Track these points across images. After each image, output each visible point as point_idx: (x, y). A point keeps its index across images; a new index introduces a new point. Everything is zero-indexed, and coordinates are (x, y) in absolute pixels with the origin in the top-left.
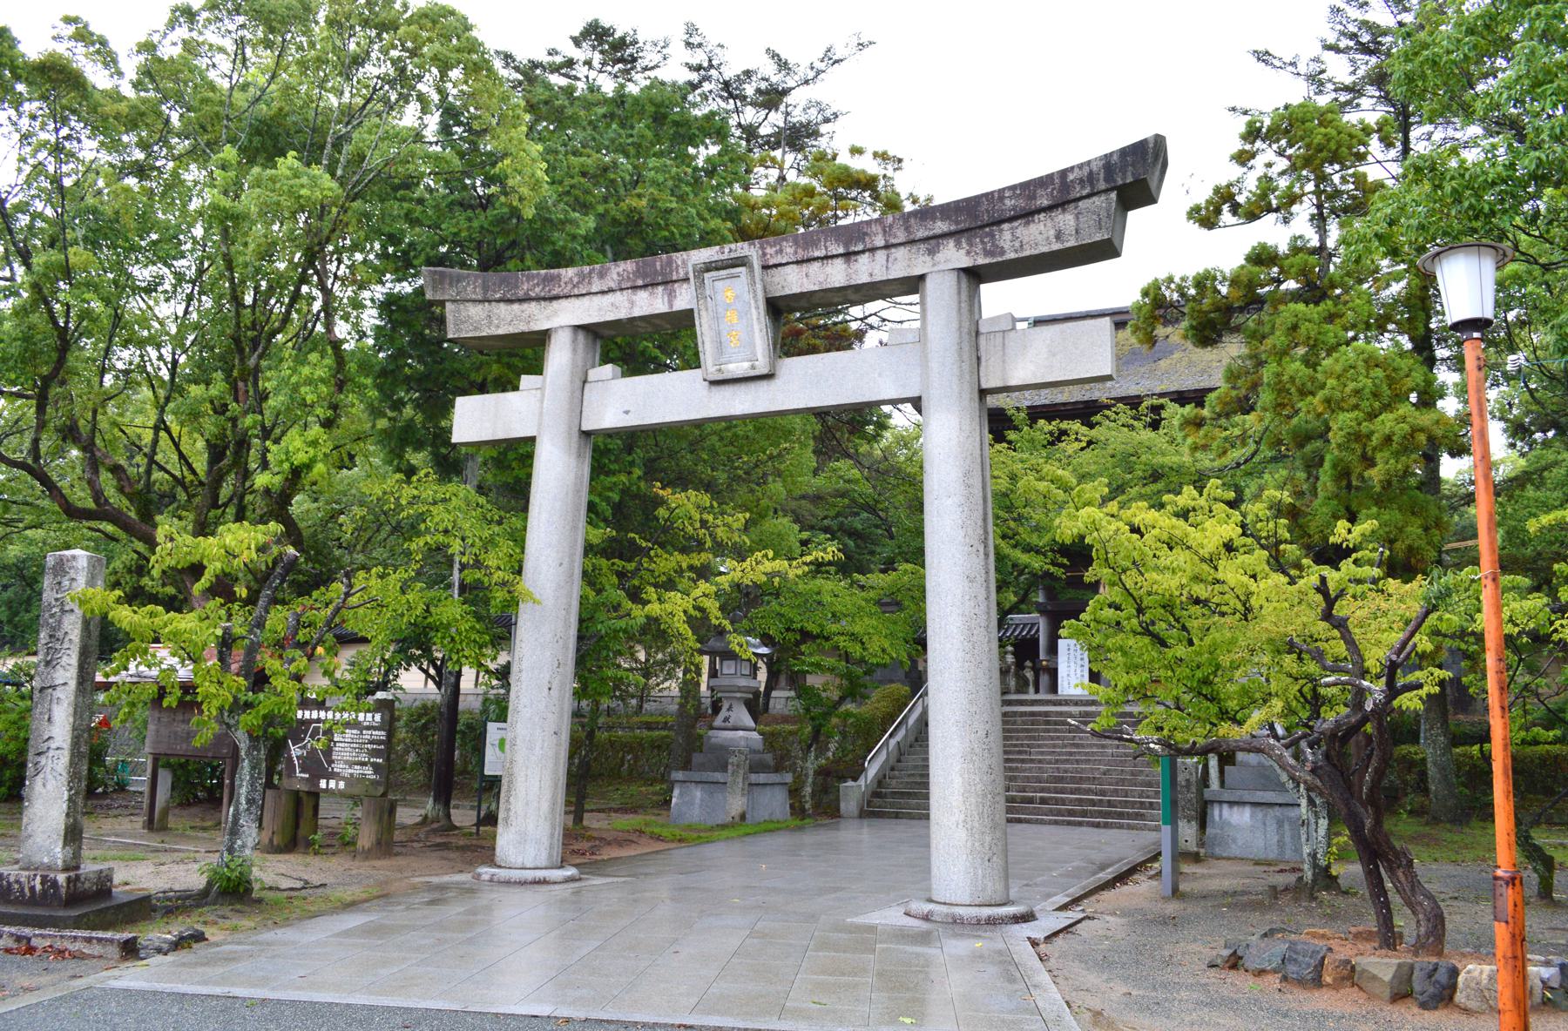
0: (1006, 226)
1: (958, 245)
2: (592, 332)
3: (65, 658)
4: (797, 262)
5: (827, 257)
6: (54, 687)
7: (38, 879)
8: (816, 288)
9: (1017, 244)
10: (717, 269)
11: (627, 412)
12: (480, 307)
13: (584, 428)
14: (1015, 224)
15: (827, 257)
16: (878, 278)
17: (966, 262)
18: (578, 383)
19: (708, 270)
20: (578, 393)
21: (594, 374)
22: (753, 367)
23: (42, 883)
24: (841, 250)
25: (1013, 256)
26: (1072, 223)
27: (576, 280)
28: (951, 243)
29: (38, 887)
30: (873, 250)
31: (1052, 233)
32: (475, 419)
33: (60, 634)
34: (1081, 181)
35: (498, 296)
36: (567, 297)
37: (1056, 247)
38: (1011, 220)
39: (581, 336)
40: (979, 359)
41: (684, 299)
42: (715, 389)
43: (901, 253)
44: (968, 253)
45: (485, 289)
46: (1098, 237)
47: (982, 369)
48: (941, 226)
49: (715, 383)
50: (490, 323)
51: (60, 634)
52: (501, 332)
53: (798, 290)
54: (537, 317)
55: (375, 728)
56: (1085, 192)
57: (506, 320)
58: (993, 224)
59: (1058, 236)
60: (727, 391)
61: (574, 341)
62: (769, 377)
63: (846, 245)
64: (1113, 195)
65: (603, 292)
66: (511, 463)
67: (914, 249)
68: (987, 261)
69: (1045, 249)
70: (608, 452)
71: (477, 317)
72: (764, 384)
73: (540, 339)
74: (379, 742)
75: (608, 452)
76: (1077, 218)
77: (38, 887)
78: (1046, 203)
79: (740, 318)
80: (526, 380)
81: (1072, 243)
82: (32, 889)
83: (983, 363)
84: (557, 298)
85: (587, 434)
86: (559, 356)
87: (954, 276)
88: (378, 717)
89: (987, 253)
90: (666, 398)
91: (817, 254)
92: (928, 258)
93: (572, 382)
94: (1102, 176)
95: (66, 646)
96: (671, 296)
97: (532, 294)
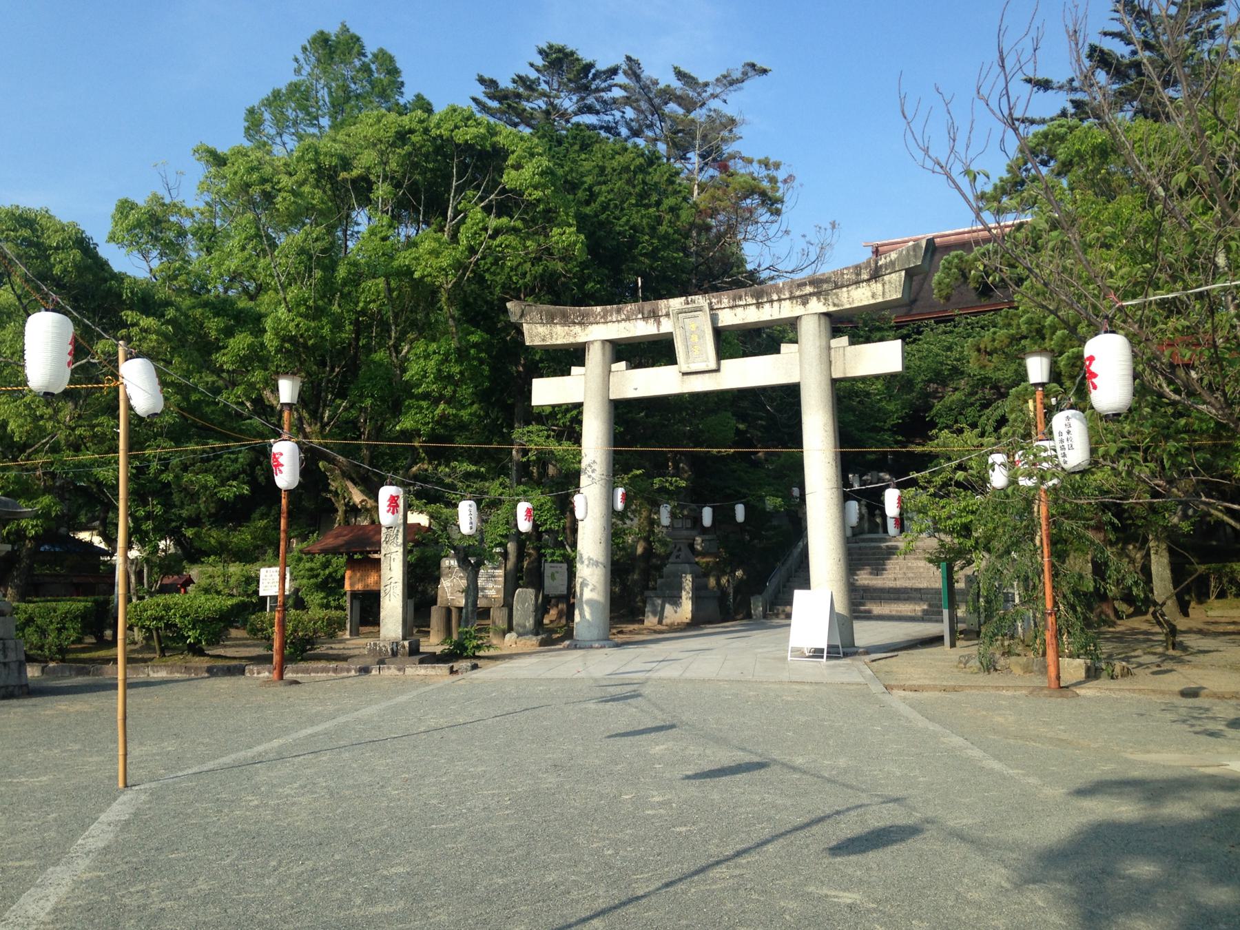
1: (819, 299)
17: (824, 310)
21: (615, 367)
25: (848, 306)
30: (772, 301)
31: (870, 294)
32: (547, 392)
37: (872, 301)
38: (847, 286)
41: (666, 326)
43: (786, 304)
48: (809, 289)
49: (684, 374)
52: (559, 342)
57: (562, 336)
61: (603, 348)
62: (717, 370)
64: (903, 273)
69: (866, 303)
70: (625, 415)
71: (541, 332)
75: (625, 415)
80: (575, 370)
81: (880, 300)
86: (595, 357)
87: (816, 317)
89: (835, 305)
96: (659, 323)
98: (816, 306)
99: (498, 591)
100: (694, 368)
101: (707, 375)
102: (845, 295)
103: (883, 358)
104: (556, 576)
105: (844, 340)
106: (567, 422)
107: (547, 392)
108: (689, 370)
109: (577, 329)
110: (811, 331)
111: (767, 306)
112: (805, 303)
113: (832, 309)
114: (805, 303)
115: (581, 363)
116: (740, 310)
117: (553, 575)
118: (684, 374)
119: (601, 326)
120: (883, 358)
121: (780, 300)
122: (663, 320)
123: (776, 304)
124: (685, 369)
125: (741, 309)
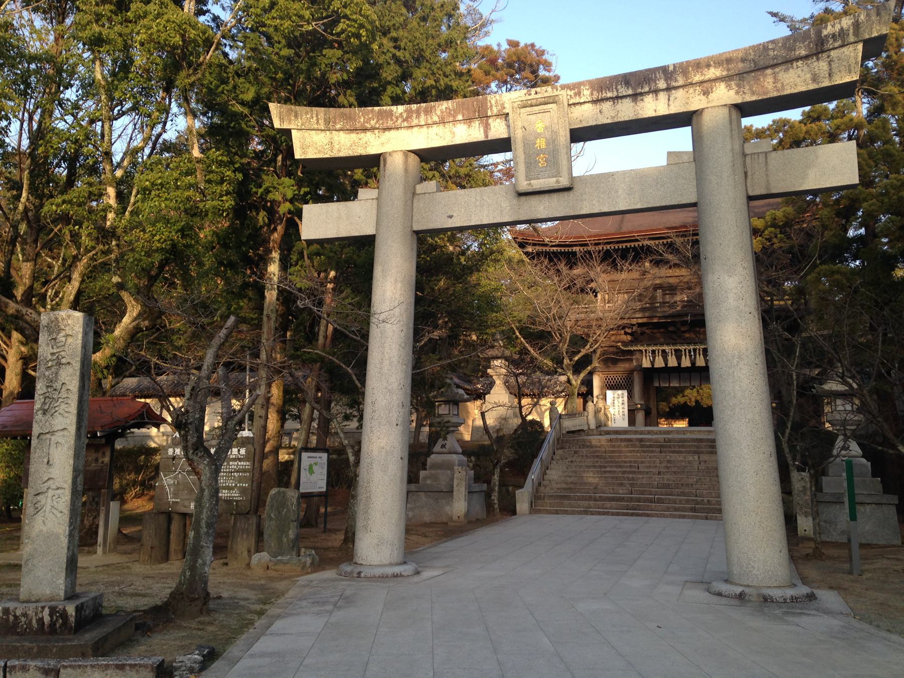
0: (769, 71)
1: (729, 87)
3: (63, 406)
5: (618, 98)
6: (52, 433)
7: (47, 611)
8: (609, 121)
9: (779, 85)
10: (532, 106)
11: (451, 217)
12: (323, 134)
13: (415, 229)
14: (777, 70)
17: (738, 100)
18: (410, 195)
19: (525, 107)
20: (409, 203)
21: (420, 188)
22: (557, 182)
23: (51, 615)
24: (630, 92)
25: (775, 94)
27: (405, 115)
29: (47, 619)
30: (656, 92)
31: (809, 76)
32: (321, 221)
33: (57, 385)
34: (834, 36)
35: (338, 126)
36: (397, 129)
37: (812, 86)
38: (773, 66)
40: (746, 173)
42: (523, 198)
43: (680, 93)
44: (737, 93)
45: (327, 122)
47: (749, 180)
48: (713, 72)
51: (57, 385)
53: (594, 123)
54: (371, 144)
55: (240, 460)
56: (837, 44)
59: (815, 79)
60: (534, 201)
63: (634, 89)
64: (860, 47)
65: (427, 125)
67: (691, 90)
68: (754, 98)
69: (804, 89)
72: (566, 194)
74: (244, 471)
76: (830, 64)
77: (47, 619)
78: (803, 53)
81: (826, 83)
82: (41, 621)
83: (749, 177)
84: (389, 129)
85: (417, 233)
88: (243, 451)
92: (703, 98)
93: (405, 193)
94: (851, 31)
95: (63, 394)
97: (368, 126)
99: (243, 491)
101: (555, 196)
102: (770, 80)
104: (315, 468)
106: (354, 259)
107: (321, 221)
112: (706, 93)
114: (706, 93)
116: (607, 105)
117: (311, 467)
118: (521, 194)
119: (403, 132)
121: (668, 89)
123: (662, 96)
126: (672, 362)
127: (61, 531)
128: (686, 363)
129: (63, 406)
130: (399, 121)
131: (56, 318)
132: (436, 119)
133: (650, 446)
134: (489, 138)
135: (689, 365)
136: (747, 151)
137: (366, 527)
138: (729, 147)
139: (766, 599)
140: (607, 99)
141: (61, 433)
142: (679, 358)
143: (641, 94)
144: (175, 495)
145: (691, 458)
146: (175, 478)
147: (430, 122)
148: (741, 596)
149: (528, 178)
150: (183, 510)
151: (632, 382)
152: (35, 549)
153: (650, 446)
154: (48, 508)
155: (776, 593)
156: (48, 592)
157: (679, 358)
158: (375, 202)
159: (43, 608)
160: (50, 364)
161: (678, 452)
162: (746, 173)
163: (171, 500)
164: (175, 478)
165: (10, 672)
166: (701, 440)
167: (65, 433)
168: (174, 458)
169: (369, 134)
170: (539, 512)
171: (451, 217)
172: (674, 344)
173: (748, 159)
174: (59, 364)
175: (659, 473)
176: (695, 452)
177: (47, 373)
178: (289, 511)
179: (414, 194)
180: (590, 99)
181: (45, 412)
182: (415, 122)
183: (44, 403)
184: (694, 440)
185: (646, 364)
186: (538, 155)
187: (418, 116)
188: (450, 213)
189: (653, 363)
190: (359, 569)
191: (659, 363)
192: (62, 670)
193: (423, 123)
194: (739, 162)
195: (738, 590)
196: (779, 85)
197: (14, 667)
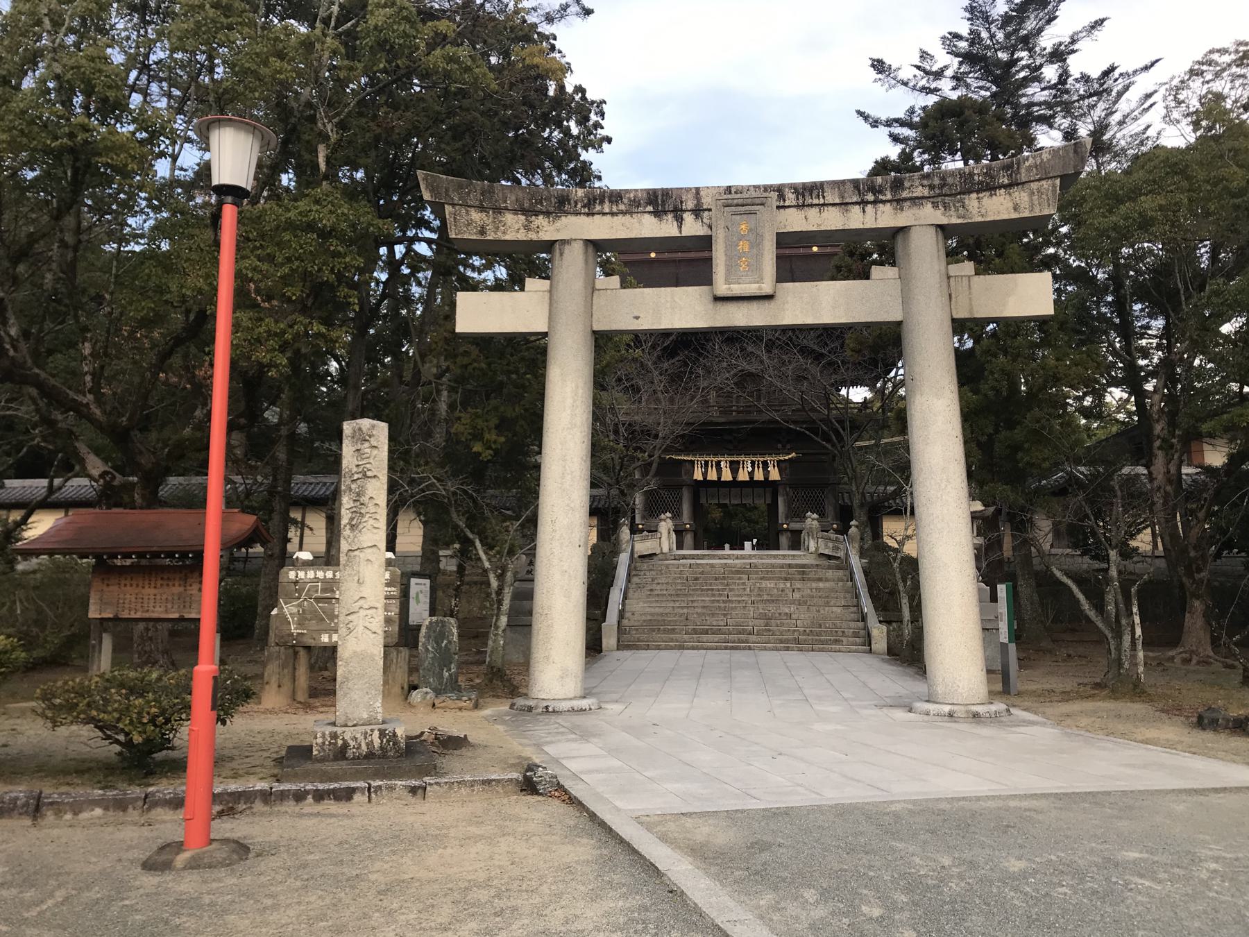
0: (974, 196)
1: (935, 205)
2: (596, 246)
4: (797, 206)
5: (824, 205)
7: (376, 733)
8: (815, 229)
10: (737, 205)
11: (637, 318)
13: (595, 328)
15: (824, 205)
16: (868, 226)
17: (944, 221)
22: (760, 288)
25: (980, 219)
26: (1026, 199)
28: (930, 205)
29: (377, 743)
31: (1011, 205)
37: (1015, 216)
38: (978, 192)
39: (591, 250)
40: (950, 295)
42: (719, 305)
46: (1046, 212)
49: (717, 299)
50: (497, 228)
51: (365, 499)
52: (508, 237)
54: (547, 230)
58: (964, 193)
59: (1016, 208)
60: (732, 308)
61: (586, 252)
62: (769, 297)
64: (1058, 182)
65: (613, 214)
66: (524, 356)
68: (959, 221)
69: (1006, 217)
70: (613, 354)
73: (549, 246)
77: (377, 743)
78: (1006, 181)
79: (751, 247)
81: (1026, 214)
85: (594, 332)
86: (572, 267)
87: (933, 230)
90: (678, 309)
91: (816, 201)
95: (372, 509)
96: (680, 220)
98: (931, 215)
100: (737, 289)
103: (1031, 295)
105: (968, 267)
106: (524, 356)
107: (481, 313)
108: (729, 294)
109: (541, 221)
110: (924, 250)
111: (857, 209)
113: (955, 220)
115: (542, 272)
116: (813, 212)
118: (717, 299)
119: (583, 218)
120: (1031, 295)
122: (688, 218)
124: (722, 288)
125: (814, 211)
126: (727, 476)
127: (376, 652)
128: (743, 476)
129: (371, 522)
130: (579, 206)
131: (360, 429)
132: (622, 207)
133: (738, 572)
134: (684, 234)
135: (762, 479)
136: (951, 274)
137: (547, 658)
138: (937, 267)
139: (976, 716)
140: (812, 206)
141: (370, 550)
142: (735, 471)
143: (847, 204)
144: (300, 624)
145: (782, 586)
146: (299, 605)
147: (615, 209)
148: (951, 715)
149: (728, 282)
150: (311, 642)
151: (681, 498)
152: (350, 672)
153: (738, 572)
154: (360, 628)
155: (980, 709)
156: (365, 716)
157: (735, 471)
158: (547, 295)
159: (372, 730)
160: (356, 477)
161: (768, 579)
162: (950, 295)
163: (294, 630)
164: (299, 605)
165: (376, 792)
166: (790, 566)
167: (374, 549)
168: (296, 582)
169: (541, 217)
170: (628, 647)
171: (637, 318)
172: (730, 455)
173: (952, 280)
174: (365, 476)
175: (753, 602)
176: (786, 579)
177: (353, 486)
178: (450, 642)
179: (594, 290)
180: (794, 203)
181: (353, 527)
182: (598, 208)
183: (352, 519)
184: (797, 566)
185: (698, 476)
186: (740, 258)
187: (602, 203)
188: (636, 314)
189: (705, 474)
190: (532, 703)
191: (712, 475)
192: (428, 788)
193: (607, 210)
194: (945, 284)
195: (947, 709)
196: (983, 211)
197: (380, 787)
